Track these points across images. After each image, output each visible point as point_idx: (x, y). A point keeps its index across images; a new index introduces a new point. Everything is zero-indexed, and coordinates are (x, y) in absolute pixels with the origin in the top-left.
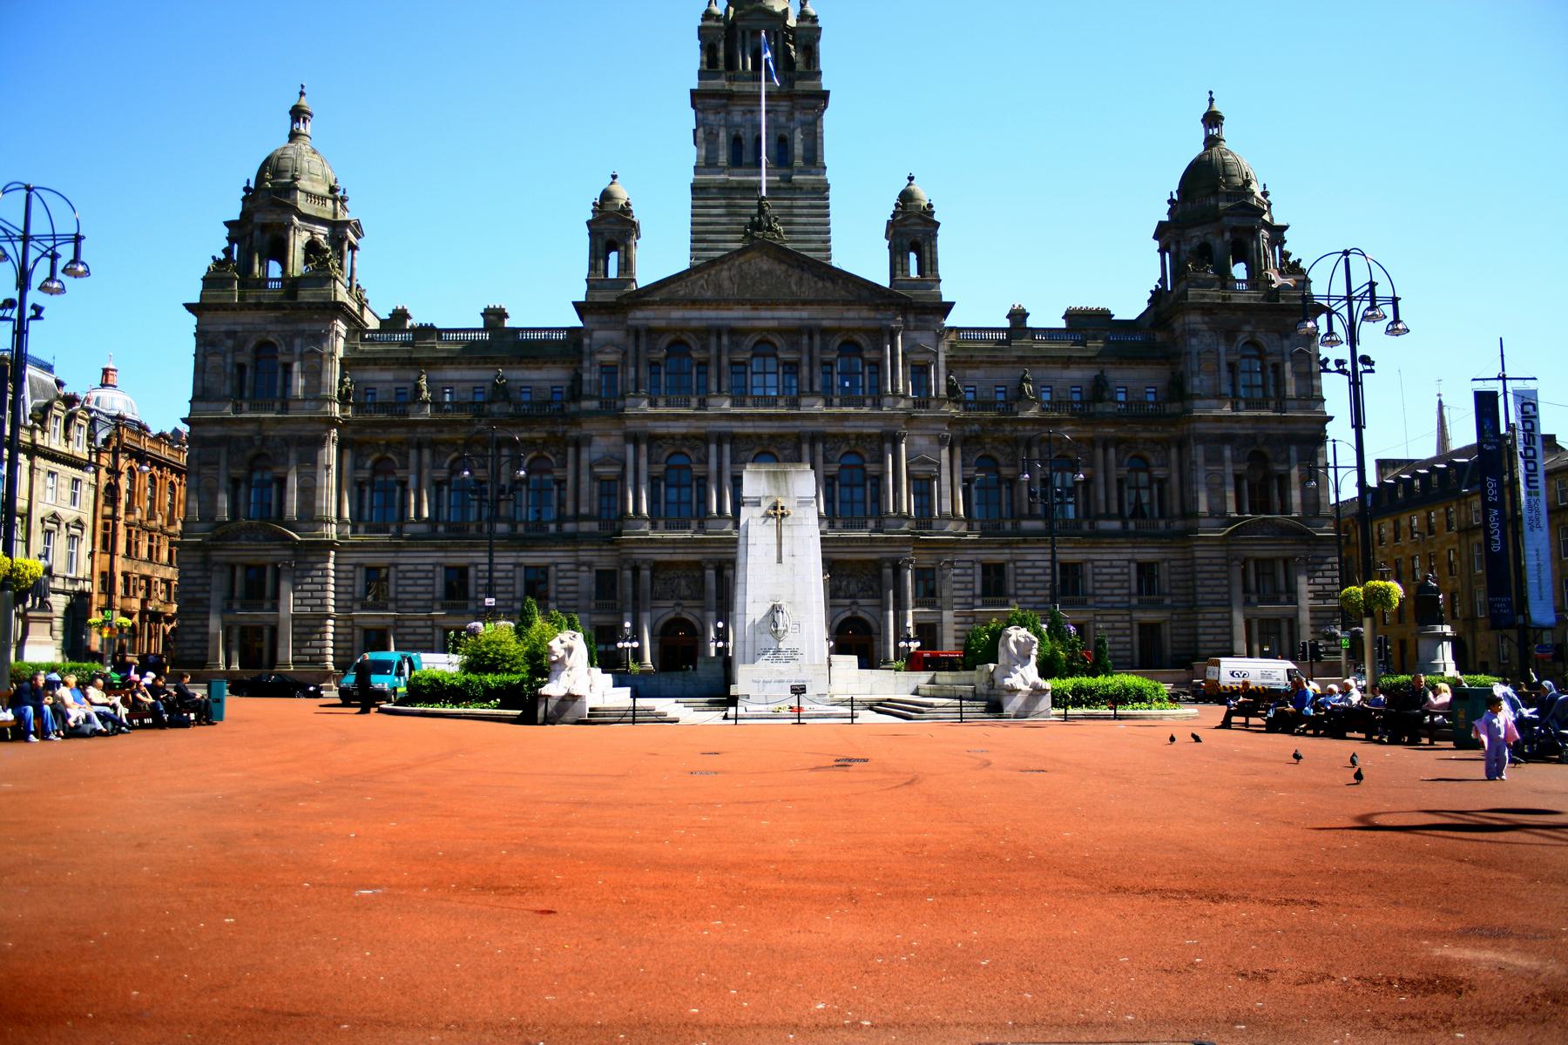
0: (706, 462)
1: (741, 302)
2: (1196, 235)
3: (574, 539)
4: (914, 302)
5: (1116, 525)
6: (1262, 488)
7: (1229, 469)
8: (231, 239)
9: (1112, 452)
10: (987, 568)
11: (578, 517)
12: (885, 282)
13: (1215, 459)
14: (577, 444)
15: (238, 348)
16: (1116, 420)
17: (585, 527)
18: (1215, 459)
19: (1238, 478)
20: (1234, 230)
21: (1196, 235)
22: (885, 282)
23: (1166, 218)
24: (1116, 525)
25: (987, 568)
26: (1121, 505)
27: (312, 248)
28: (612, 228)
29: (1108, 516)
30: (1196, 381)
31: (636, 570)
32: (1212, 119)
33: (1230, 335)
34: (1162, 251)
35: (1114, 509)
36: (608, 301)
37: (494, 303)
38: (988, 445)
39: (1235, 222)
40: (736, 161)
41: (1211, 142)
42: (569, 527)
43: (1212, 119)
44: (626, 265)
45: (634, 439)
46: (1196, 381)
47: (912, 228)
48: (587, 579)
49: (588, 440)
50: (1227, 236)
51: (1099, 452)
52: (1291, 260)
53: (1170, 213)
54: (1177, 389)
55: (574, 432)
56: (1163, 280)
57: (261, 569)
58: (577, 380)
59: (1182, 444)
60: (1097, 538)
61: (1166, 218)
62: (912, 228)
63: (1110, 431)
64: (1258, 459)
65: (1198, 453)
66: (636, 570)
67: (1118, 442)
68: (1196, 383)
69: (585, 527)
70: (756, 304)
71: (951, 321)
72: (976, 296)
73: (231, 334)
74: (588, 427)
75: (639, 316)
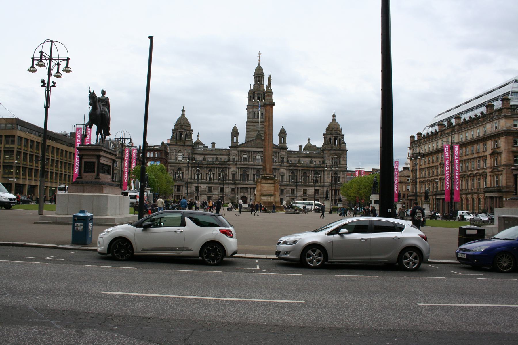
1: (255, 147)
3: (228, 184)
4: (282, 147)
8: (173, 133)
10: (292, 189)
11: (229, 180)
14: (229, 168)
15: (176, 151)
17: (230, 181)
19: (332, 177)
21: (329, 136)
23: (325, 132)
25: (292, 189)
27: (186, 134)
28: (235, 132)
31: (238, 188)
36: (234, 146)
37: (213, 142)
38: (293, 170)
40: (254, 117)
44: (237, 140)
45: (238, 168)
48: (230, 190)
49: (231, 168)
54: (323, 162)
55: (228, 166)
57: (180, 186)
58: (229, 158)
59: (324, 171)
60: (309, 186)
65: (326, 173)
66: (238, 188)
67: (314, 170)
68: (326, 162)
69: (230, 181)
70: (257, 148)
71: (288, 150)
72: (293, 146)
73: (175, 149)
74: (231, 166)
75: (239, 149)
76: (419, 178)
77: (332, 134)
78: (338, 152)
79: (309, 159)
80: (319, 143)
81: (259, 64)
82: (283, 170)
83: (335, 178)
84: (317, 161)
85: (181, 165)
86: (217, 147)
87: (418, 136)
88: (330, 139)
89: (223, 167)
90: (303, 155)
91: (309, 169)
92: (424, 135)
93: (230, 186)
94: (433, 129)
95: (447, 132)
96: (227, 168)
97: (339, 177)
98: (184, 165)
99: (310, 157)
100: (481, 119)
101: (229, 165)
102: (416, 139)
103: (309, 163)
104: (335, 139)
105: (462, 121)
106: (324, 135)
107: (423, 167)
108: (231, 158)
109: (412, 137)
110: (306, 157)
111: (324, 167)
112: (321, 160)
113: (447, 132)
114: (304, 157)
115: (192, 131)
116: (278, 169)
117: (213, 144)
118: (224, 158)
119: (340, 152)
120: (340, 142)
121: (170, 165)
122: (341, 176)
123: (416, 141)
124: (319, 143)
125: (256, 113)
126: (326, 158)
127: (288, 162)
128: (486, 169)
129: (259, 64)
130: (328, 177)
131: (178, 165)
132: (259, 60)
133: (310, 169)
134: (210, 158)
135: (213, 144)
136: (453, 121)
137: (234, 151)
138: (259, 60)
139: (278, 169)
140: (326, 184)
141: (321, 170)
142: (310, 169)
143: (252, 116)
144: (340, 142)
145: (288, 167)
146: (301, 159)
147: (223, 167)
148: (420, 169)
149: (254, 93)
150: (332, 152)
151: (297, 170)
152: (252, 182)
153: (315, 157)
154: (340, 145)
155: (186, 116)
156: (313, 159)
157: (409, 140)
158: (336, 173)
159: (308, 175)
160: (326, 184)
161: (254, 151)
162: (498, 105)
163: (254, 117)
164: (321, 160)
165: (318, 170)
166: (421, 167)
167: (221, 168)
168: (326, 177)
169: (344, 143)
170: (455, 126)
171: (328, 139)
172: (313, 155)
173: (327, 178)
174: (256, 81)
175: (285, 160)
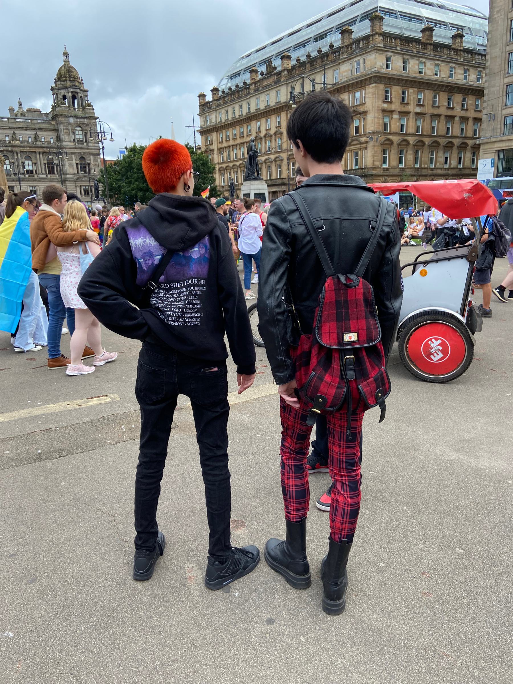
2: (62, 92)
5: (44, 176)
7: (74, 162)
9: (41, 155)
13: (70, 159)
19: (77, 164)
20: (72, 92)
21: (62, 92)
24: (44, 176)
26: (46, 171)
29: (43, 174)
30: (63, 137)
32: (66, 54)
34: (53, 95)
35: (44, 172)
39: (72, 90)
46: (63, 137)
50: (70, 94)
51: (38, 155)
52: (89, 102)
53: (55, 83)
56: (55, 103)
61: (54, 85)
63: (41, 150)
64: (82, 158)
67: (43, 153)
76: (219, 164)
77: (67, 88)
78: (82, 120)
80: (45, 104)
84: (47, 138)
87: (213, 94)
88: (64, 97)
90: (21, 125)
91: (33, 150)
92: (223, 92)
94: (239, 81)
95: (265, 83)
97: (89, 164)
99: (34, 129)
100: (330, 57)
102: (209, 98)
104: (74, 98)
105: (220, 93)
106: (52, 89)
107: (225, 144)
110: (26, 129)
111: (61, 148)
113: (265, 83)
114: (21, 128)
119: (86, 121)
120: (82, 104)
122: (92, 163)
123: (209, 102)
124: (45, 104)
126: (62, 132)
128: (271, 154)
130: (71, 165)
133: (37, 150)
136: (277, 63)
140: (68, 176)
142: (37, 150)
144: (82, 104)
146: (16, 132)
148: (219, 149)
150: (72, 120)
151: (12, 152)
153: (41, 129)
154: (84, 108)
156: (39, 133)
157: (196, 102)
160: (68, 176)
162: (362, 29)
164: (54, 134)
166: (220, 146)
168: (66, 163)
169: (90, 105)
170: (280, 73)
171: (61, 96)
172: (38, 126)
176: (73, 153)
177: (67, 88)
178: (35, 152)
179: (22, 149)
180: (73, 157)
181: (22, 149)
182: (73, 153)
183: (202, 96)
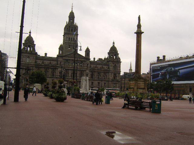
0: (69, 72)
6: (115, 77)
7: (112, 75)
12: (84, 56)
13: (111, 74)
16: (104, 70)
18: (111, 74)
21: (111, 54)
22: (84, 56)
32: (114, 43)
33: (113, 64)
38: (93, 71)
41: (114, 45)
42: (56, 76)
43: (114, 43)
47: (88, 51)
49: (58, 69)
54: (109, 68)
59: (109, 73)
62: (88, 51)
64: (115, 74)
65: (110, 74)
68: (110, 68)
73: (25, 56)
75: (64, 58)
79: (101, 66)
81: (72, 10)
82: (88, 71)
83: (115, 77)
85: (29, 65)
86: (48, 56)
89: (54, 68)
93: (58, 79)
96: (56, 68)
98: (31, 65)
99: (102, 65)
101: (58, 67)
102: (161, 58)
103: (101, 68)
108: (59, 63)
109: (158, 58)
110: (100, 65)
112: (107, 67)
115: (35, 45)
116: (85, 71)
117: (46, 54)
118: (54, 63)
121: (22, 65)
123: (161, 59)
125: (71, 38)
127: (90, 66)
129: (72, 10)
130: (111, 76)
131: (27, 65)
132: (72, 8)
134: (47, 62)
135: (46, 54)
137: (60, 59)
138: (72, 8)
139: (85, 71)
141: (107, 72)
143: (68, 39)
145: (90, 69)
147: (54, 68)
149: (70, 26)
152: (71, 77)
155: (32, 36)
156: (103, 66)
157: (156, 59)
158: (115, 74)
159: (94, 74)
161: (72, 60)
163: (69, 41)
164: (107, 67)
165: (106, 72)
167: (53, 68)
173: (111, 77)
174: (70, 20)
175: (89, 66)
176: (112, 73)
177: (113, 53)
178: (101, 72)
179: (98, 71)
180: (112, 74)
181: (98, 71)
182: (112, 73)
183: (158, 58)
